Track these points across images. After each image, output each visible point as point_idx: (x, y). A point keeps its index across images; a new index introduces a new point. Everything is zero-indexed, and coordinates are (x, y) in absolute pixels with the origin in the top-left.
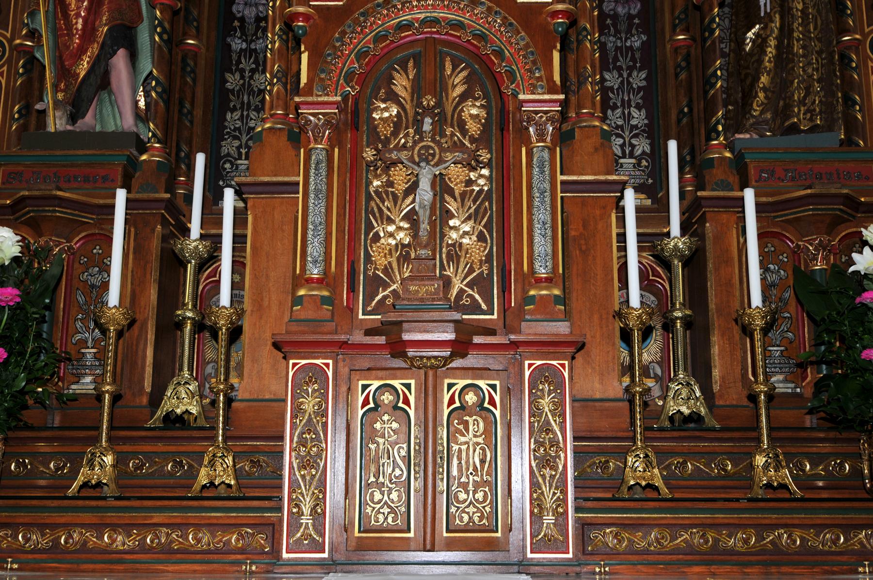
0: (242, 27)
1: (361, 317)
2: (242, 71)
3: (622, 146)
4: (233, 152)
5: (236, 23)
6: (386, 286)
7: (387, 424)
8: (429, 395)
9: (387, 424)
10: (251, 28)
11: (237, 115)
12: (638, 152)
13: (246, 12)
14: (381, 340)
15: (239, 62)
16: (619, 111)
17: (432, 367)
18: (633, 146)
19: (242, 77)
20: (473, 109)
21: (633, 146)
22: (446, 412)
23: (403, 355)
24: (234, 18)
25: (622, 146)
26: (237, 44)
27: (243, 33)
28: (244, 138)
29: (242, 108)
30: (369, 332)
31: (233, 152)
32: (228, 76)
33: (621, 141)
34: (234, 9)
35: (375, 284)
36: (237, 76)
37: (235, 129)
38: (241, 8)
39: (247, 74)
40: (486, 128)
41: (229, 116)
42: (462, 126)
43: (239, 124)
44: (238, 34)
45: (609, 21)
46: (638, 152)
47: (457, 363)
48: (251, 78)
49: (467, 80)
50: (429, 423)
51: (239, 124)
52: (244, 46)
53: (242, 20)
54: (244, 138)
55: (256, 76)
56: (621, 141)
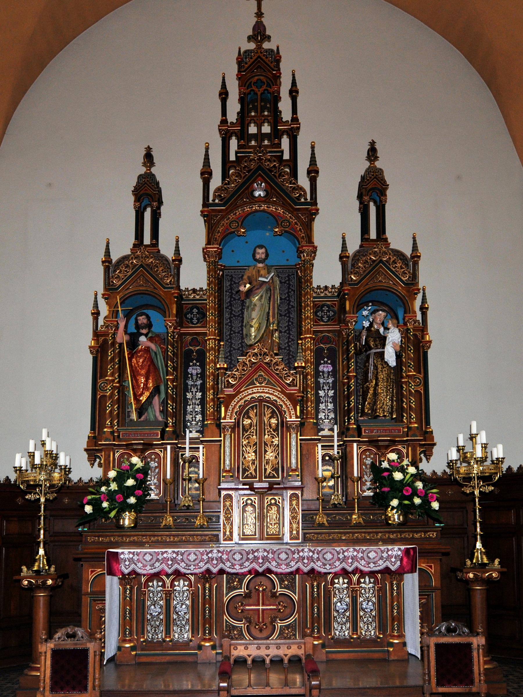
0: (192, 377)
1: (241, 480)
2: (192, 392)
3: (325, 416)
4: (191, 420)
5: (190, 376)
6: (248, 471)
7: (249, 509)
8: (261, 502)
9: (249, 509)
10: (195, 377)
11: (191, 406)
12: (330, 418)
13: (193, 372)
14: (248, 487)
15: (191, 389)
16: (324, 404)
17: (262, 494)
18: (328, 416)
19: (192, 394)
20: (274, 421)
21: (328, 416)
22: (266, 505)
23: (254, 491)
24: (189, 374)
25: (325, 416)
26: (190, 383)
27: (192, 379)
28: (194, 414)
29: (193, 404)
30: (243, 485)
31: (191, 420)
32: (187, 394)
33: (324, 414)
34: (189, 370)
35: (245, 470)
36: (191, 393)
37: (191, 412)
38: (191, 370)
39: (194, 393)
40: (277, 425)
41: (188, 407)
42: (270, 425)
43: (192, 410)
44: (190, 379)
45: (321, 374)
46: (330, 418)
47: (269, 492)
48: (195, 394)
49: (272, 413)
50: (261, 507)
51: (192, 410)
52: (193, 383)
53: (192, 374)
54: (194, 414)
55: (197, 394)
56: (324, 414)
